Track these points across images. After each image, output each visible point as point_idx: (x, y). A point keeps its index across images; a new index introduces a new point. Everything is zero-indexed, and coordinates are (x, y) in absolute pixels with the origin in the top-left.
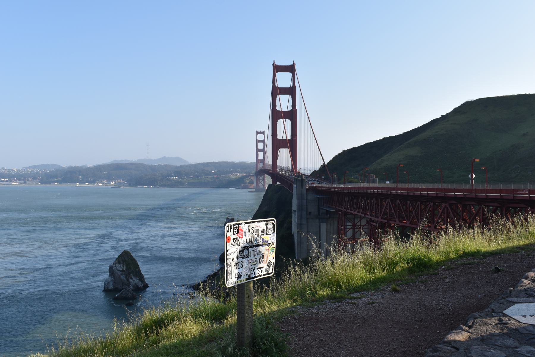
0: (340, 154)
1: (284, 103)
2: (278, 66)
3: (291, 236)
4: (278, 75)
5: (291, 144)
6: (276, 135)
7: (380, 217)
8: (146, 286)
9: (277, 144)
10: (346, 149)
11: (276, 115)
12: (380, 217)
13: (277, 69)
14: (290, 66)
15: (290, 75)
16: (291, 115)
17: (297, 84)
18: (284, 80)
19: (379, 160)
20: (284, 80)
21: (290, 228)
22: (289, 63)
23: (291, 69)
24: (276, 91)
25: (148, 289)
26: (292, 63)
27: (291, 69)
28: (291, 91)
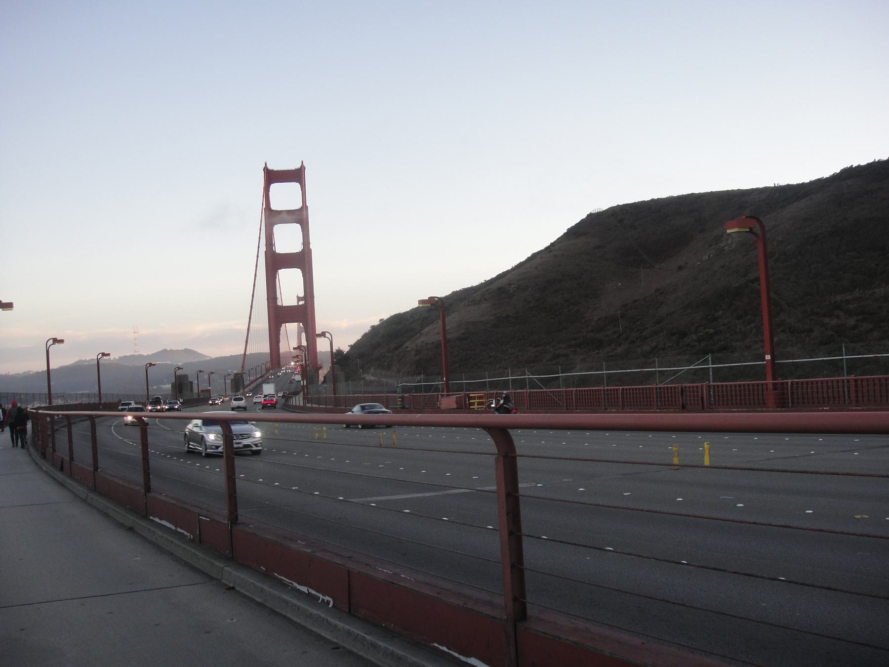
0: (373, 327)
1: (288, 239)
2: (272, 171)
5: (303, 313)
6: (275, 299)
9: (279, 315)
11: (275, 262)
13: (272, 177)
14: (296, 170)
15: (296, 186)
16: (301, 260)
18: (285, 196)
22: (294, 166)
26: (299, 166)
27: (296, 176)
28: (300, 216)
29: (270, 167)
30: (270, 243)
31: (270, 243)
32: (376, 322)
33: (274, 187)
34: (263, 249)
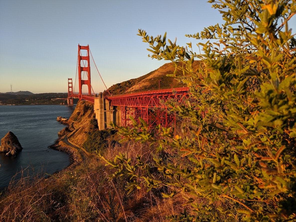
0: (112, 86)
1: (84, 64)
3: (96, 121)
4: (82, 51)
5: (88, 82)
7: (147, 106)
8: (22, 148)
9: (82, 82)
10: (115, 84)
11: (81, 69)
12: (147, 106)
13: (80, 47)
17: (90, 55)
18: (84, 53)
19: (131, 88)
20: (84, 53)
21: (95, 117)
23: (87, 48)
24: (81, 58)
25: (23, 151)
26: (87, 46)
27: (87, 48)
28: (88, 58)
29: (80, 45)
30: (80, 65)
31: (80, 65)
32: (112, 85)
33: (81, 50)
34: (78, 66)
